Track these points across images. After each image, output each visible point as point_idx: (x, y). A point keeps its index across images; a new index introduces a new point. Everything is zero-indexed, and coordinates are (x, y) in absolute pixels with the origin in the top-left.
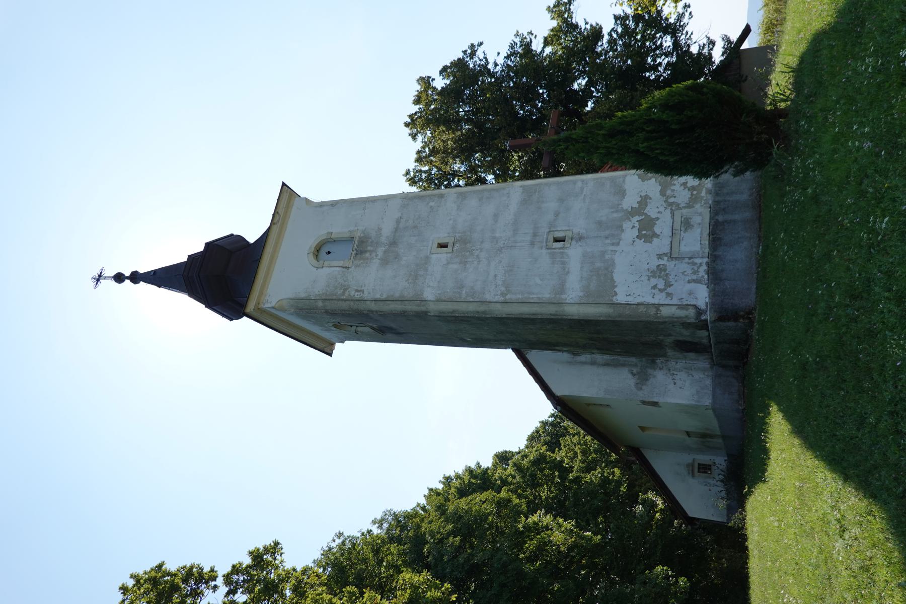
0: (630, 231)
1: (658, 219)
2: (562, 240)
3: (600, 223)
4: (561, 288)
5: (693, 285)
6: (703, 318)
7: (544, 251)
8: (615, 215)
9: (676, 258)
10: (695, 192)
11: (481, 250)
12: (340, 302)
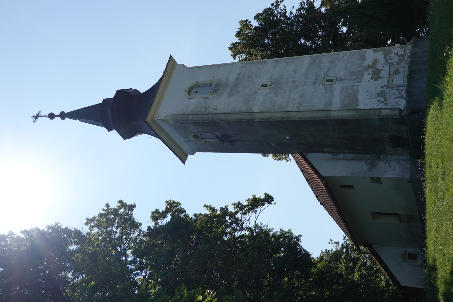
0: (367, 76)
1: (382, 70)
2: (331, 81)
3: (352, 73)
4: (330, 103)
5: (398, 99)
6: (403, 114)
7: (321, 87)
8: (360, 69)
9: (390, 87)
10: (402, 57)
11: (286, 87)
12: (203, 115)
